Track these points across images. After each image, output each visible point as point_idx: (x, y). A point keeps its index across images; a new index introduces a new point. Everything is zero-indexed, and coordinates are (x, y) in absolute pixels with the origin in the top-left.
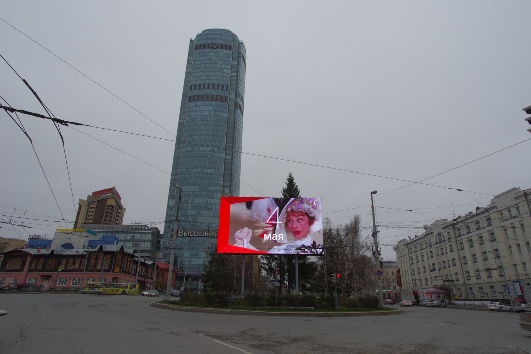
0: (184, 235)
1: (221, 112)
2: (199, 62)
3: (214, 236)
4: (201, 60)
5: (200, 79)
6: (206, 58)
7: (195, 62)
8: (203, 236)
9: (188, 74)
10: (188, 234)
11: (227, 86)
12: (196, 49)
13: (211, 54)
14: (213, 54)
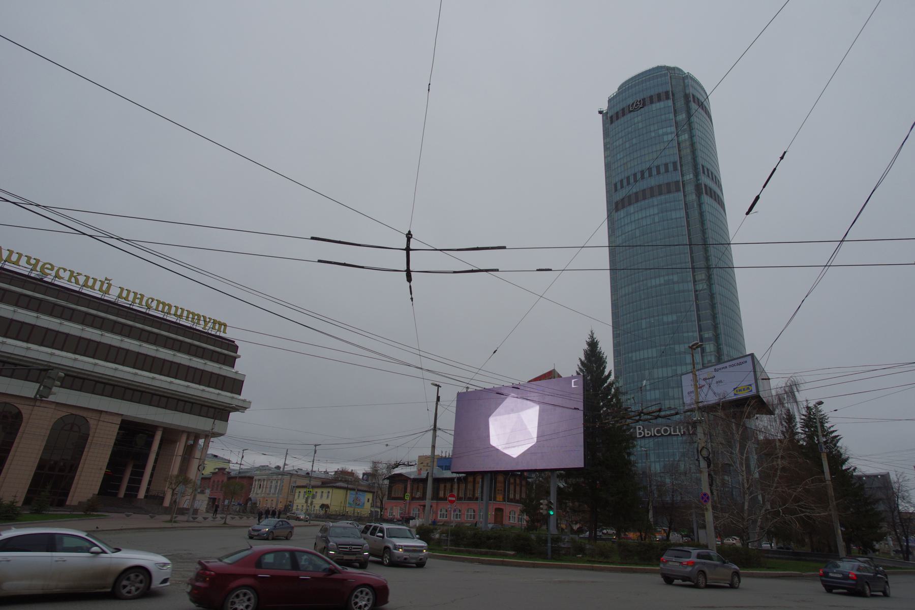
0: (646, 435)
1: (671, 211)
2: (621, 141)
4: (622, 137)
5: (626, 168)
6: (630, 129)
7: (615, 144)
8: (678, 433)
9: (608, 166)
11: (675, 164)
12: (612, 122)
13: (636, 120)
14: (640, 118)
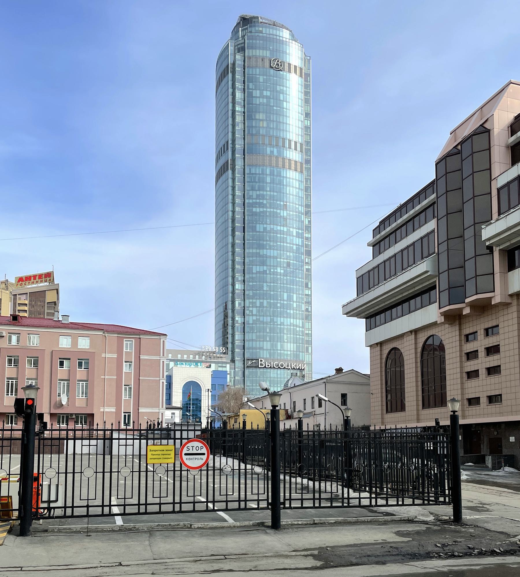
0: (267, 367)
3: (301, 369)
8: (290, 368)
10: (271, 365)
